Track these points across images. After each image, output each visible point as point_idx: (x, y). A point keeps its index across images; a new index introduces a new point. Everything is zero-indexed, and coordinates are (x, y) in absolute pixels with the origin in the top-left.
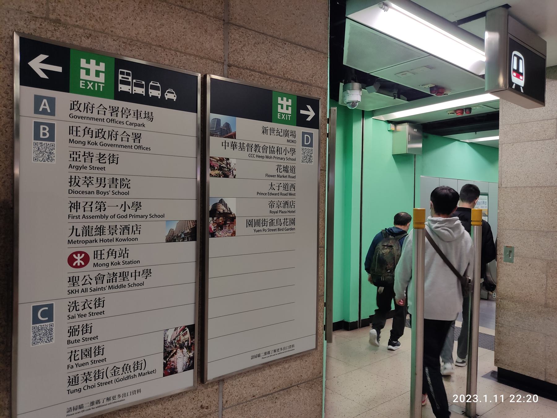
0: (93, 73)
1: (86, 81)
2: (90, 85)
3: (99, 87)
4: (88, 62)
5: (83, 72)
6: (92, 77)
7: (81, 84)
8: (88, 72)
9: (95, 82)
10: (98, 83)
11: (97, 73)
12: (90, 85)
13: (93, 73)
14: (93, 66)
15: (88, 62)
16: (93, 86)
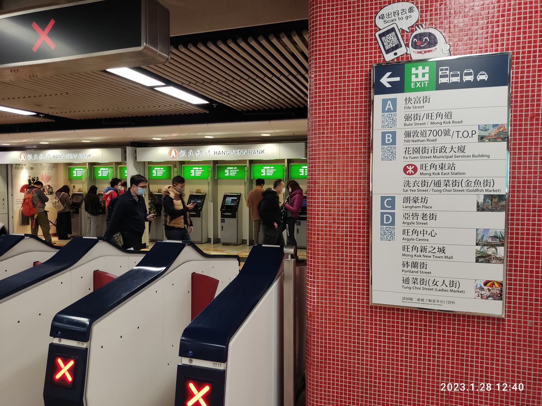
0: (420, 75)
1: (415, 82)
2: (418, 85)
3: (424, 84)
4: (417, 69)
5: (413, 77)
6: (420, 78)
9: (421, 82)
10: (424, 81)
12: (418, 85)
13: (420, 75)
15: (417, 69)
16: (421, 84)
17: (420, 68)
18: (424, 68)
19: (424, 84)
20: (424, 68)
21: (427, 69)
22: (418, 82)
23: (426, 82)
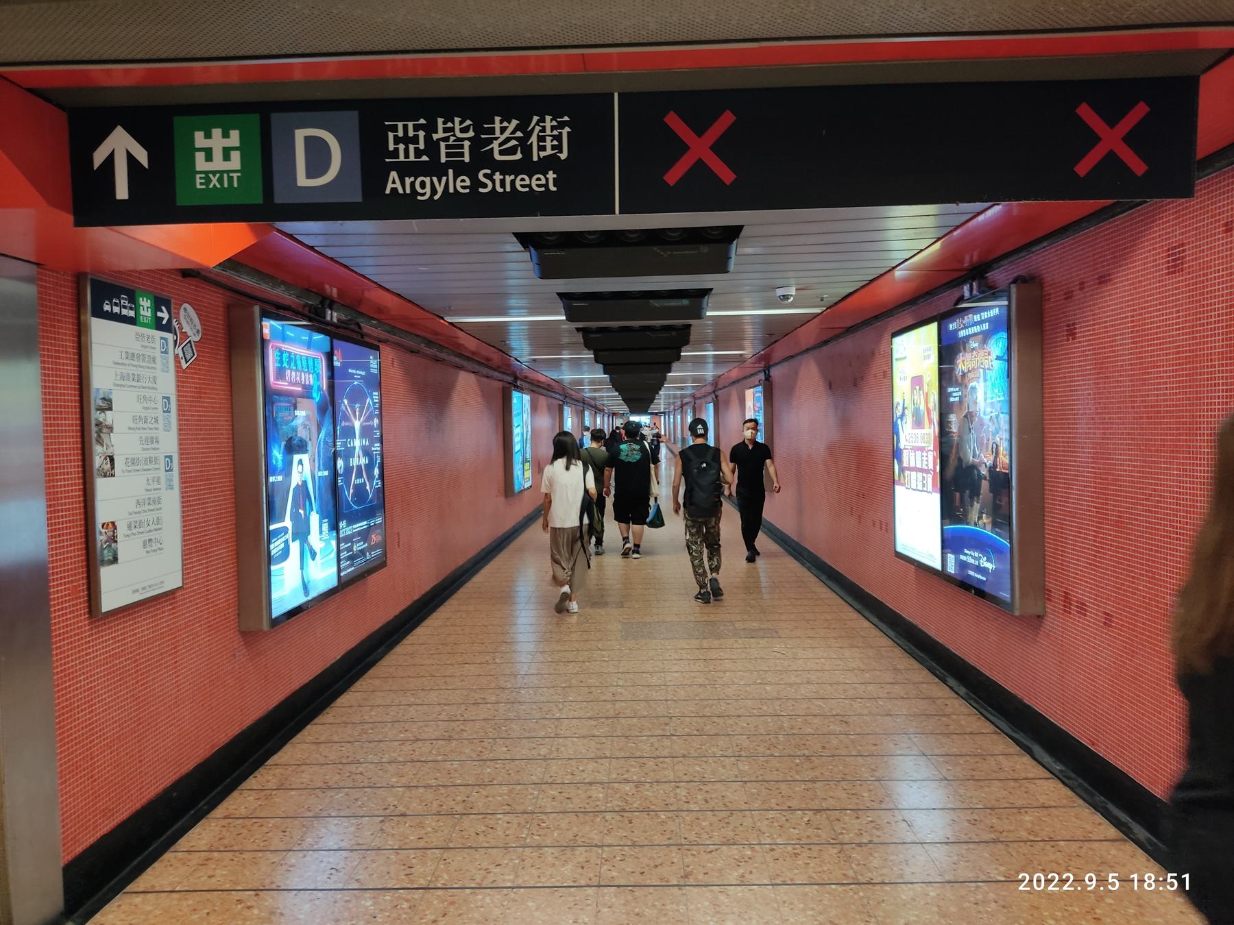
0: (218, 155)
2: (214, 181)
3: (230, 179)
4: (208, 136)
5: (200, 157)
6: (218, 164)
7: (198, 181)
8: (209, 158)
9: (222, 172)
10: (228, 172)
11: (227, 157)
12: (214, 181)
13: (218, 155)
14: (217, 141)
15: (208, 136)
16: (220, 180)
17: (217, 132)
18: (226, 135)
19: (230, 179)
20: (226, 135)
21: (235, 135)
22: (214, 173)
23: (235, 175)
